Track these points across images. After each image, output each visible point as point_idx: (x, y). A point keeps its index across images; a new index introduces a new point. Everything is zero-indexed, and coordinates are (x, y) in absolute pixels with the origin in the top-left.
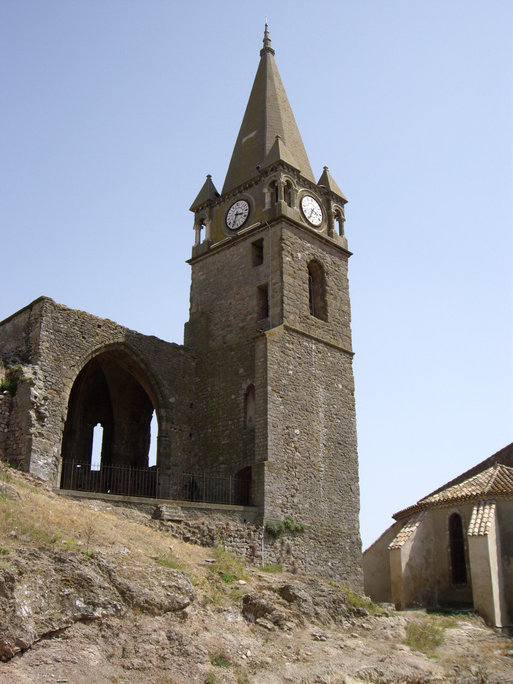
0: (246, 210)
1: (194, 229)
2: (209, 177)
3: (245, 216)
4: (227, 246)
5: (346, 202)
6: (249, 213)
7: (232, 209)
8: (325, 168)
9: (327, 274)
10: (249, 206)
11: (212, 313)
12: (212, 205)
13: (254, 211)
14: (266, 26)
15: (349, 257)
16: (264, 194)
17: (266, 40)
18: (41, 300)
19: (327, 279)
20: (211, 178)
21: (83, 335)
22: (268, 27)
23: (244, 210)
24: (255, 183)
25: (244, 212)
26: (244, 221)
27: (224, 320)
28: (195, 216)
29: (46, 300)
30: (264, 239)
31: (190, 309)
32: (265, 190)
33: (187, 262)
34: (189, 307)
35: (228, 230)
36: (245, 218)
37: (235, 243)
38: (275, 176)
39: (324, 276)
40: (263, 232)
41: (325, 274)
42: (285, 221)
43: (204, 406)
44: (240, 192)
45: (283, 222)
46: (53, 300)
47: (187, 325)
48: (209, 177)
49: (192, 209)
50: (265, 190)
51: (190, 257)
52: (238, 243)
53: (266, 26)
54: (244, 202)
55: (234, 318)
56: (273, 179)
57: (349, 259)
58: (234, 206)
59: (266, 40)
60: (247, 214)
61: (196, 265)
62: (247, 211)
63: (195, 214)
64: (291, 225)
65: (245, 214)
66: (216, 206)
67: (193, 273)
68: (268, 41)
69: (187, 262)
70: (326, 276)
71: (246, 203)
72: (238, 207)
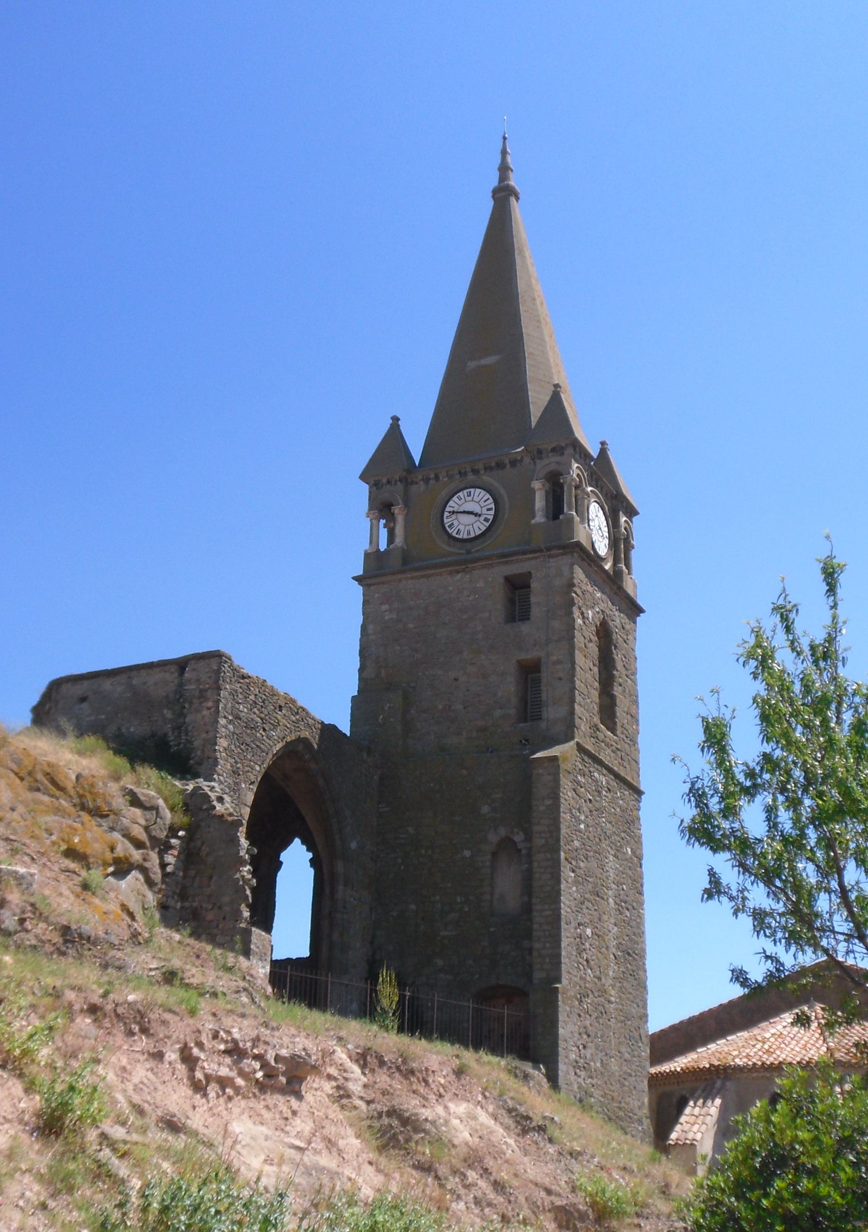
0: (489, 510)
1: (368, 517)
2: (396, 419)
3: (486, 520)
4: (449, 569)
5: (636, 513)
6: (496, 516)
7: (455, 498)
8: (603, 443)
9: (616, 647)
10: (496, 502)
11: (414, 688)
12: (409, 480)
13: (506, 516)
14: (505, 138)
15: (639, 615)
16: (533, 492)
17: (504, 169)
18: (217, 656)
19: (615, 657)
20: (400, 423)
21: (264, 725)
22: (507, 141)
23: (484, 509)
24: (510, 462)
25: (484, 511)
26: (483, 528)
27: (440, 707)
28: (370, 492)
29: (224, 658)
30: (533, 575)
31: (361, 670)
32: (537, 485)
33: (355, 578)
34: (358, 665)
35: (446, 537)
36: (487, 524)
37: (467, 567)
38: (558, 463)
39: (611, 650)
40: (533, 562)
41: (613, 647)
42: (578, 553)
43: (400, 861)
44: (475, 472)
45: (575, 554)
46: (233, 659)
47: (354, 698)
48: (396, 419)
49: (364, 477)
50: (537, 485)
51: (360, 572)
52: (473, 569)
53: (505, 138)
54: (483, 492)
55: (465, 708)
56: (553, 467)
57: (638, 619)
58: (461, 494)
59: (504, 169)
60: (491, 517)
61: (372, 588)
62: (492, 512)
63: (370, 488)
64: (583, 560)
65: (488, 517)
66: (416, 483)
67: (366, 603)
68: (510, 172)
69: (354, 578)
70: (614, 651)
71: (488, 496)
72: (470, 498)
